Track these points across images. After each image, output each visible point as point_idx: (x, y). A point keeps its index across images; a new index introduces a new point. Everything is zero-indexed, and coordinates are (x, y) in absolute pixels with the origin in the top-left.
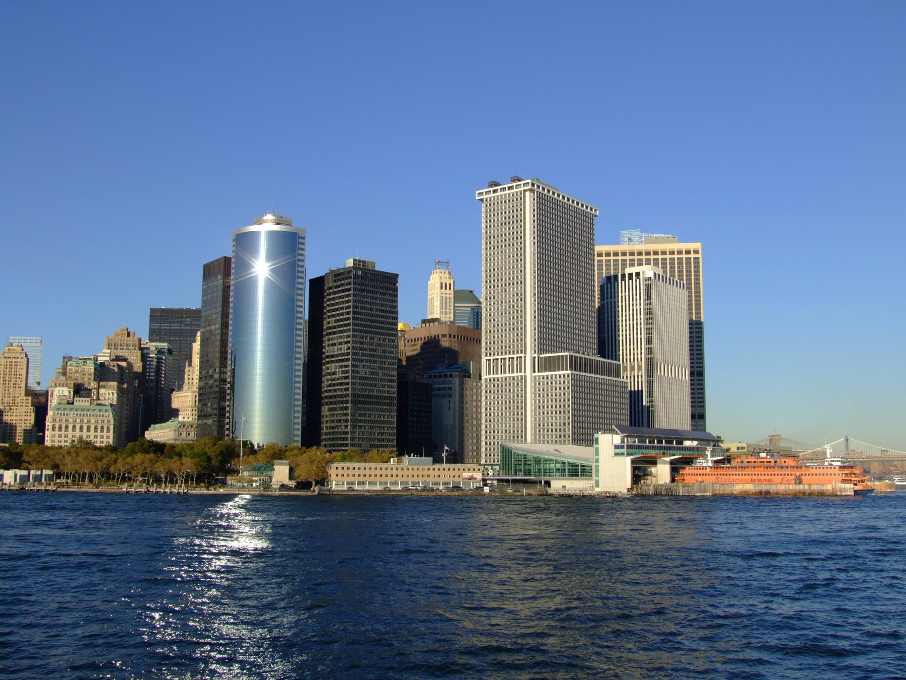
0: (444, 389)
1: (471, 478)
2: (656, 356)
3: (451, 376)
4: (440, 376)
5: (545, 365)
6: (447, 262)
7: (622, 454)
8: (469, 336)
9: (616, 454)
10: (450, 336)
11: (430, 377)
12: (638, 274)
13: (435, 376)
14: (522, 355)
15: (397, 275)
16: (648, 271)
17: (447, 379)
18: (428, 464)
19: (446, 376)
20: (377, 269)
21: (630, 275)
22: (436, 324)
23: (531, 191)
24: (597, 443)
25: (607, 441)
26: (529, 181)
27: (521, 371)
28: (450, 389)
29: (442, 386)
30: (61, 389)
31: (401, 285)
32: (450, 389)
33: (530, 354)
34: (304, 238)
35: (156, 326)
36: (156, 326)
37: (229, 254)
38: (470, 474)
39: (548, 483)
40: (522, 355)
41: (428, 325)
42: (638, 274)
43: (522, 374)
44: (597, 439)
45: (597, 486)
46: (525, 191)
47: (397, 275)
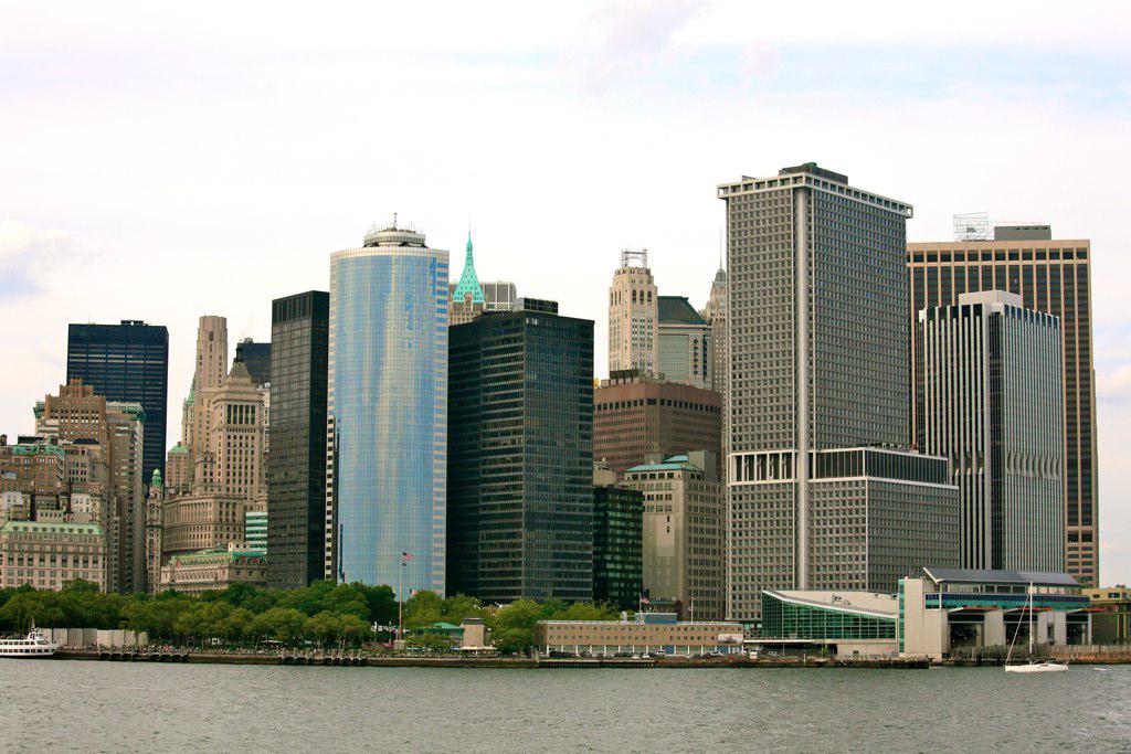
2: (1008, 443)
3: (671, 476)
4: (653, 477)
5: (826, 465)
6: (644, 253)
8: (694, 402)
9: (928, 607)
10: (662, 402)
11: (635, 477)
12: (978, 308)
13: (644, 477)
14: (793, 451)
15: (593, 322)
16: (993, 300)
17: (664, 482)
19: (662, 476)
20: (561, 313)
21: (966, 309)
22: (636, 380)
23: (808, 191)
24: (902, 592)
25: (914, 588)
27: (789, 476)
28: (669, 497)
30: (12, 494)
32: (669, 497)
34: (446, 266)
35: (81, 357)
36: (81, 357)
37: (325, 288)
38: (728, 635)
39: (833, 648)
41: (621, 381)
42: (978, 308)
43: (792, 480)
44: (902, 587)
46: (795, 190)
47: (593, 322)
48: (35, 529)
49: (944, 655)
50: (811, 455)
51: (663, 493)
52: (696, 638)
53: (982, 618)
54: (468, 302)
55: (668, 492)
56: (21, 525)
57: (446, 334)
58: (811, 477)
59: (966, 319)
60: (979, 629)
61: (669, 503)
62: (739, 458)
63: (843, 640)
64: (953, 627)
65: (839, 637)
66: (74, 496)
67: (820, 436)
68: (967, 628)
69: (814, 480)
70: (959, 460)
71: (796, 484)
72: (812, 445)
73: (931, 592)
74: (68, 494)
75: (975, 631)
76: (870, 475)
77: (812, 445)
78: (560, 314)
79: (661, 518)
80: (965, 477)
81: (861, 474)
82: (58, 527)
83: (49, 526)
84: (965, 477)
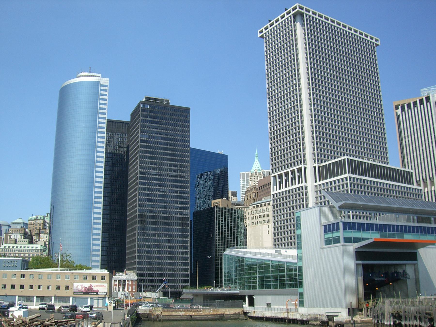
0: (264, 216)
1: (88, 292)
4: (261, 206)
7: (337, 240)
9: (328, 242)
11: (254, 207)
14: (302, 166)
18: (15, 267)
26: (297, 5)
28: (268, 215)
29: (262, 214)
31: (193, 117)
33: (310, 165)
38: (87, 285)
40: (302, 166)
43: (303, 184)
45: (302, 303)
48: (17, 247)
49: (352, 312)
50: (315, 167)
51: (266, 213)
52: (27, 287)
53: (413, 257)
54: (256, 172)
55: (268, 213)
56: (11, 246)
57: (105, 121)
58: (316, 181)
59: (422, 106)
60: (410, 271)
61: (268, 218)
62: (275, 177)
63: (258, 290)
64: (366, 268)
65: (254, 287)
66: (41, 235)
67: (320, 155)
68: (391, 270)
69: (318, 183)
70: (426, 183)
71: (306, 187)
72: (315, 162)
73: (330, 220)
74: (39, 234)
75: (405, 275)
76: (352, 173)
77: (315, 162)
78: (170, 104)
79: (265, 226)
80: (431, 191)
81: (345, 173)
82: (23, 246)
83: (23, 246)
84: (431, 191)
